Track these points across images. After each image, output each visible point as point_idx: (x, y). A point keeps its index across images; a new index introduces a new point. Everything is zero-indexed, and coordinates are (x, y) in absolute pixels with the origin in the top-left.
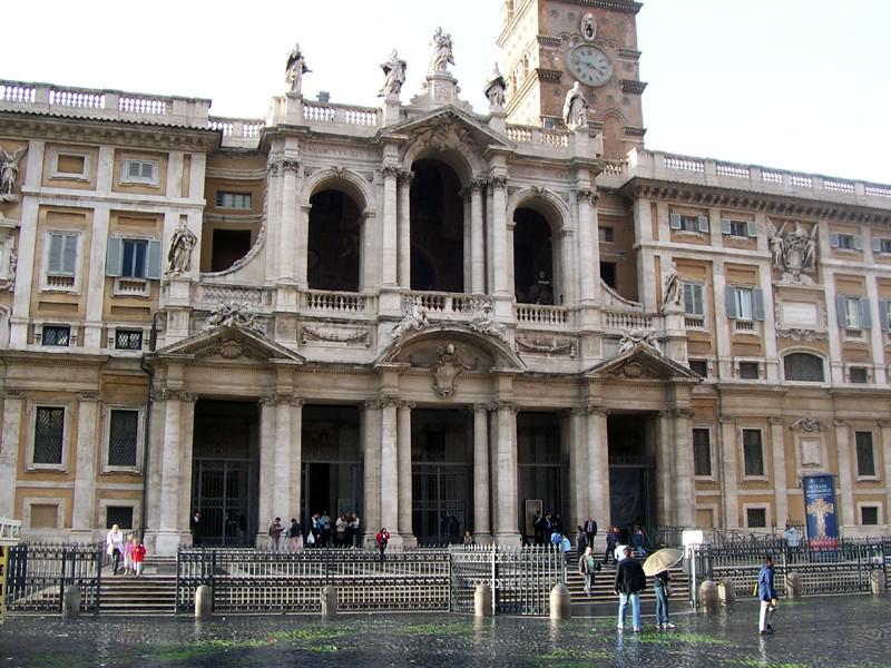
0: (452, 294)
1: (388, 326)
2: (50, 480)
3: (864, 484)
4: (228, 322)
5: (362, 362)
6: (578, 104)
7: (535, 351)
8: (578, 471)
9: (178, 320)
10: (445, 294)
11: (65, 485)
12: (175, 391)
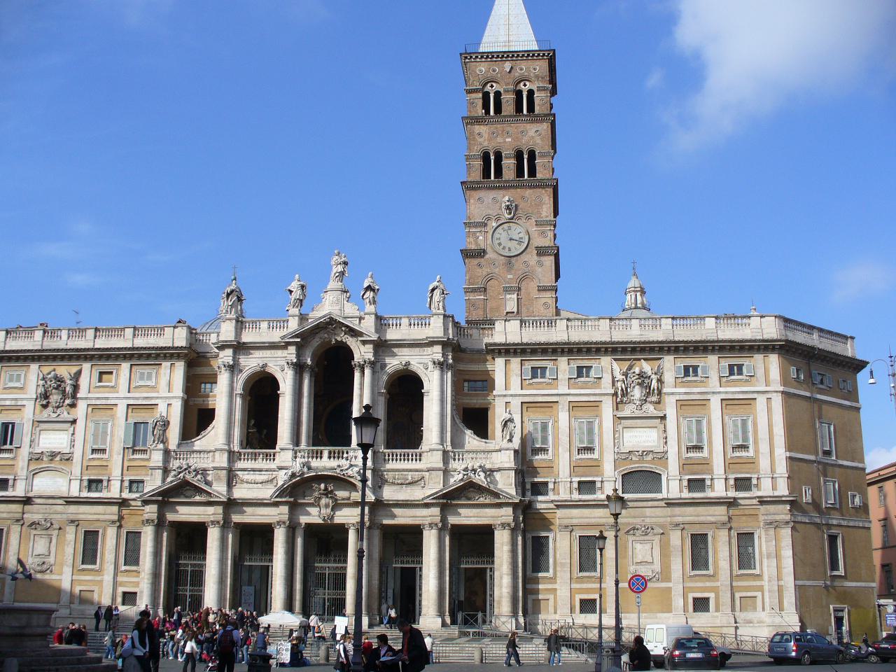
0: (328, 448)
2: (90, 575)
3: (697, 578)
4: (182, 475)
6: (437, 292)
11: (98, 578)
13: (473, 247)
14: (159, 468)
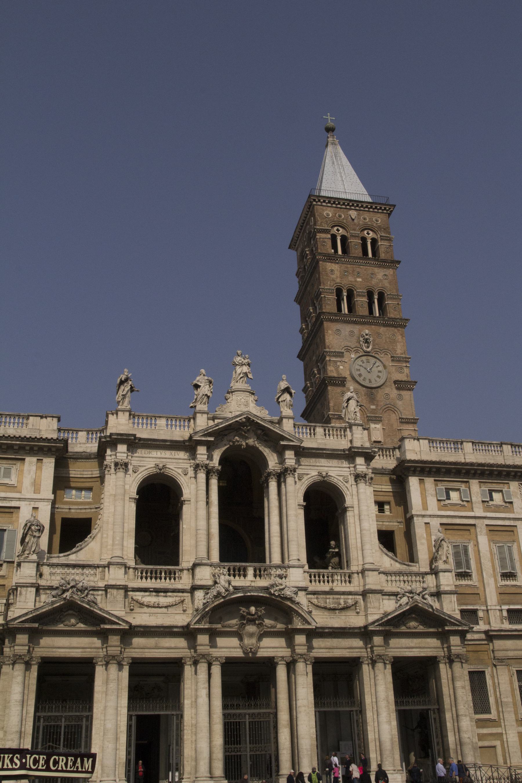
0: (253, 564)
1: (199, 594)
4: (67, 595)
5: (180, 624)
6: (352, 403)
7: (325, 608)
8: (369, 715)
9: (26, 594)
10: (247, 564)
12: (20, 656)
13: (335, 375)
14: (32, 585)
